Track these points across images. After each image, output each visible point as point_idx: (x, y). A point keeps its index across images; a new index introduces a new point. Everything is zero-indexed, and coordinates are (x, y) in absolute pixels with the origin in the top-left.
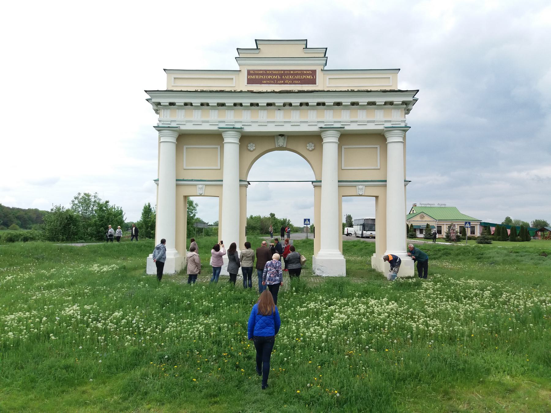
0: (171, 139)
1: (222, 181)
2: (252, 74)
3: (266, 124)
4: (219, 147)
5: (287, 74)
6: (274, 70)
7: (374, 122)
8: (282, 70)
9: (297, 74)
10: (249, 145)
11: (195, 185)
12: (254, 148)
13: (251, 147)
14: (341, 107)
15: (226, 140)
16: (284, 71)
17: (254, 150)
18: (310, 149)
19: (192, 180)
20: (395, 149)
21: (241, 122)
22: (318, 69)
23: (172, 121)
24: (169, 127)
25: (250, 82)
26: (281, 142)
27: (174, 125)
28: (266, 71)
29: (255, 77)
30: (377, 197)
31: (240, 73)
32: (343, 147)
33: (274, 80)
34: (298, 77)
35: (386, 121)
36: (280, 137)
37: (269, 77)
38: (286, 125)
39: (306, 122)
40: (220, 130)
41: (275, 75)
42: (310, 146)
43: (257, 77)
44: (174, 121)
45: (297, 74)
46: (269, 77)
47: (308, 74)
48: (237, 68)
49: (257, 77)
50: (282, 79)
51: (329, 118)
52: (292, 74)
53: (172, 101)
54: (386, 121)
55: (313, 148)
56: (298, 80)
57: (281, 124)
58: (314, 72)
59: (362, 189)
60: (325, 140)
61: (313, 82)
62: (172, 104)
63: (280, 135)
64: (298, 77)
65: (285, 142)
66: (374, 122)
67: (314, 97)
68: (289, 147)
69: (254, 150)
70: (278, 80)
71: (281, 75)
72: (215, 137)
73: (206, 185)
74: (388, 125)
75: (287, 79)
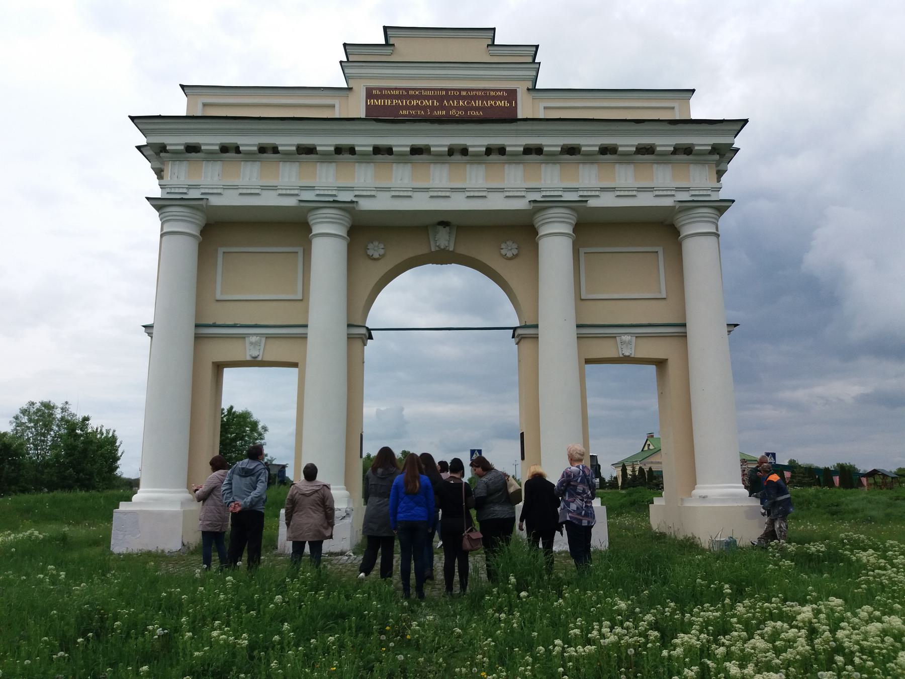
1: (306, 326)
2: (377, 97)
3: (409, 194)
4: (300, 250)
5: (454, 98)
6: (425, 89)
7: (651, 189)
8: (442, 90)
9: (475, 98)
10: (370, 246)
11: (243, 337)
12: (382, 252)
13: (376, 249)
14: (578, 157)
15: (316, 230)
16: (447, 90)
17: (382, 256)
18: (509, 255)
19: (234, 326)
20: (698, 253)
21: (351, 189)
22: (521, 88)
23: (190, 187)
24: (182, 199)
26: (443, 240)
27: (194, 194)
28: (407, 90)
30: (661, 364)
31: (352, 97)
32: (582, 251)
34: (479, 103)
35: (678, 189)
36: (441, 228)
37: (414, 103)
38: (455, 196)
39: (501, 190)
40: (302, 204)
41: (428, 98)
42: (509, 249)
43: (388, 102)
44: (196, 187)
46: (414, 103)
47: (500, 98)
49: (388, 102)
51: (551, 180)
52: (464, 98)
54: (678, 189)
55: (515, 252)
57: (443, 194)
58: (512, 95)
59: (630, 343)
60: (543, 231)
62: (192, 149)
64: (479, 103)
65: (453, 239)
66: (651, 189)
67: (518, 133)
68: (462, 250)
69: (382, 256)
71: (440, 99)
73: (268, 337)
74: (685, 196)
75: (454, 107)
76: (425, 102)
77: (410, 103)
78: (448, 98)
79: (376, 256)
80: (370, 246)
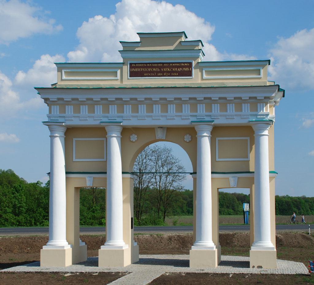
5: (165, 67)
10: (131, 137)
13: (134, 138)
16: (163, 63)
18: (188, 141)
25: (133, 74)
28: (146, 64)
32: (217, 139)
33: (153, 72)
37: (149, 70)
41: (155, 67)
46: (149, 70)
48: (121, 61)
50: (161, 72)
56: (176, 72)
61: (189, 74)
63: (159, 127)
70: (157, 72)
71: (160, 68)
77: (148, 70)
79: (134, 141)
80: (131, 137)
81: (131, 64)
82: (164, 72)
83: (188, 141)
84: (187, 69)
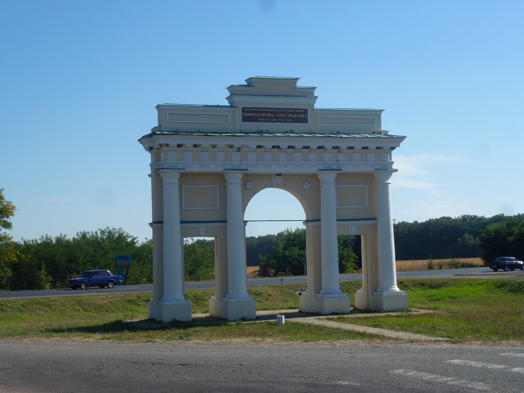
0: (172, 180)
2: (247, 112)
5: (280, 113)
16: (278, 109)
18: (307, 188)
25: (245, 119)
28: (260, 108)
29: (251, 115)
33: (268, 117)
36: (277, 177)
37: (263, 115)
41: (270, 112)
42: (306, 186)
43: (252, 115)
45: (291, 113)
46: (263, 115)
47: (301, 113)
49: (252, 115)
50: (275, 117)
52: (283, 112)
53: (180, 143)
56: (291, 118)
58: (306, 111)
61: (305, 120)
63: (277, 175)
70: (271, 118)
71: (274, 113)
72: (220, 178)
76: (268, 115)
78: (278, 113)
80: (247, 184)
81: (243, 109)
82: (279, 118)
83: (307, 188)
84: (303, 116)
